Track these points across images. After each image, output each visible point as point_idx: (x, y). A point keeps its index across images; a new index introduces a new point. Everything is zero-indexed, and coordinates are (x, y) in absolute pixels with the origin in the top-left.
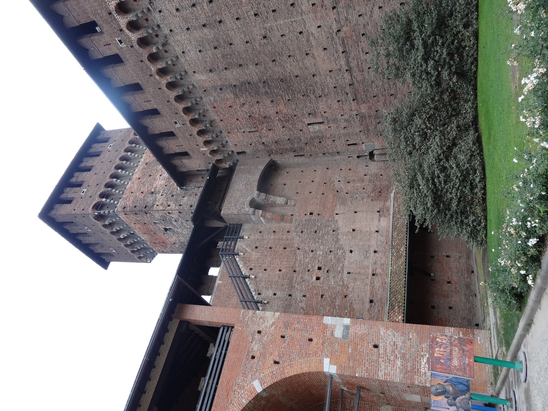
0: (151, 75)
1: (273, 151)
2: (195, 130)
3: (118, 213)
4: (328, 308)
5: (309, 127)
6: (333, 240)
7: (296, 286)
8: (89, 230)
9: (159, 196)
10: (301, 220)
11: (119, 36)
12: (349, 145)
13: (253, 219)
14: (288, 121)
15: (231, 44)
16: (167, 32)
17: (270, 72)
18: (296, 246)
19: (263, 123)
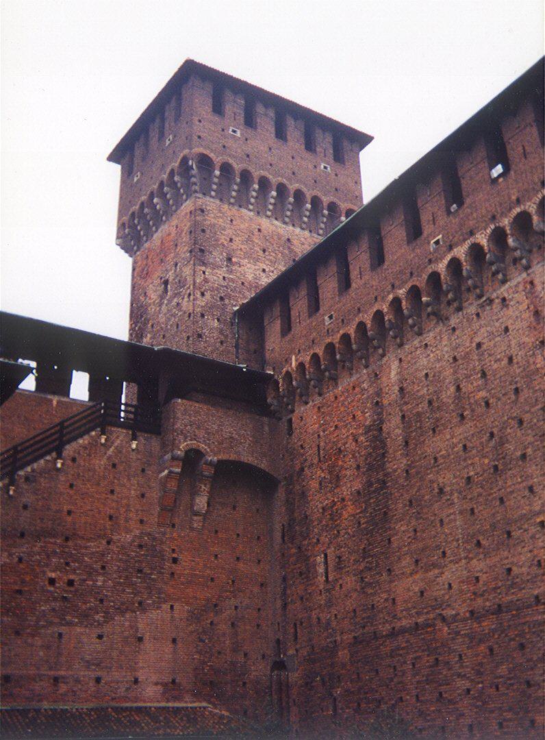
0: (393, 286)
2: (320, 351)
5: (323, 556)
6: (123, 604)
7: (39, 545)
8: (168, 142)
10: (162, 543)
12: (295, 624)
13: (166, 457)
14: (332, 519)
15: (434, 430)
16: (454, 321)
18: (115, 538)
19: (330, 473)
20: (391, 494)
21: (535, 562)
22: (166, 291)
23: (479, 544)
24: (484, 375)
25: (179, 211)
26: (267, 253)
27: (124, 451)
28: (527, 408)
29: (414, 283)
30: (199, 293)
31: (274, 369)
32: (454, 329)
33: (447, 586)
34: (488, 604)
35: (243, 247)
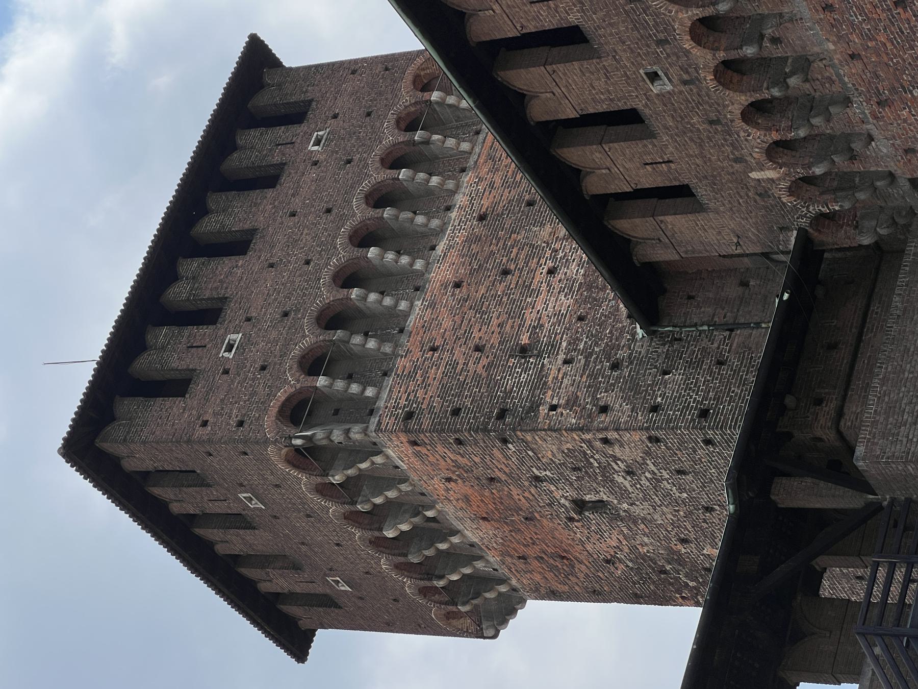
2: (736, 102)
3: (382, 438)
8: (256, 504)
9: (553, 366)
22: (599, 506)
25: (413, 476)
26: (512, 267)
30: (602, 417)
35: (495, 322)
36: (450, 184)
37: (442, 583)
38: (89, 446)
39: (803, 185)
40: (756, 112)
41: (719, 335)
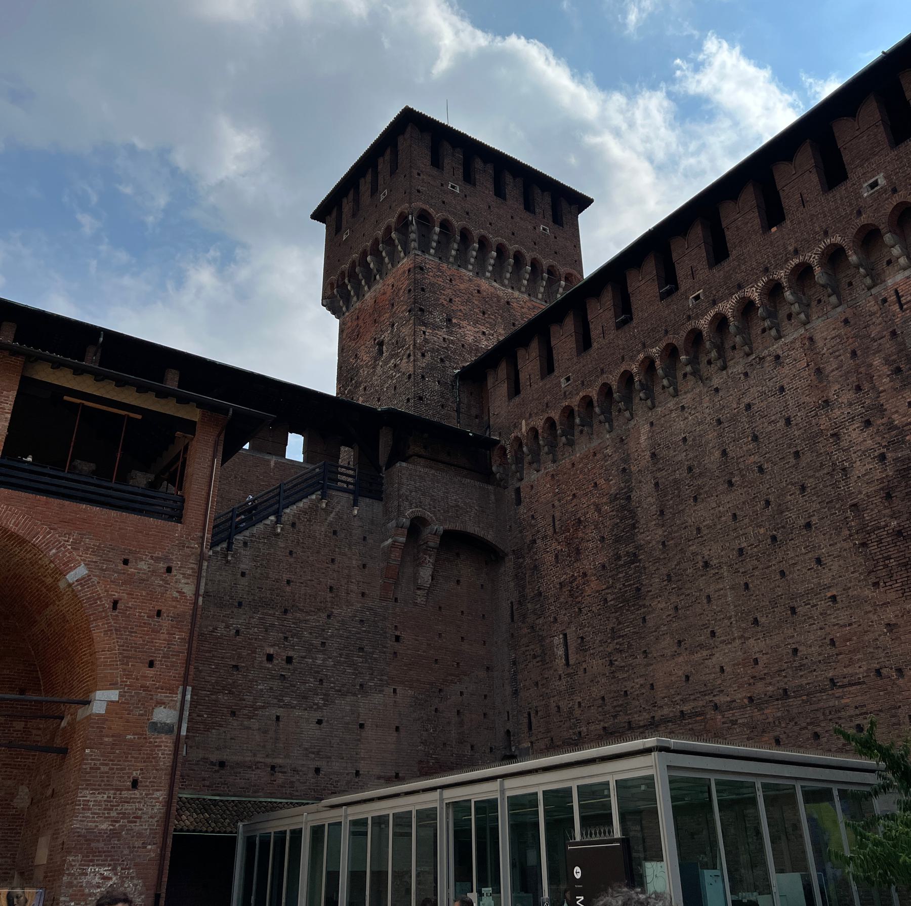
1: (521, 560)
2: (556, 415)
3: (412, 256)
4: (213, 680)
8: (382, 197)
9: (442, 333)
11: (706, 297)
13: (390, 525)
14: (571, 596)
15: (695, 499)
17: (652, 568)
18: (335, 611)
20: (645, 568)
21: (827, 641)
22: (381, 352)
23: (756, 622)
24: (755, 438)
25: (395, 270)
27: (345, 517)
28: (811, 473)
29: (669, 341)
31: (500, 434)
32: (717, 390)
33: (718, 670)
34: (770, 688)
35: (462, 308)
36: (523, 289)
37: (346, 281)
38: (410, 122)
39: (518, 441)
40: (550, 422)
41: (455, 406)
